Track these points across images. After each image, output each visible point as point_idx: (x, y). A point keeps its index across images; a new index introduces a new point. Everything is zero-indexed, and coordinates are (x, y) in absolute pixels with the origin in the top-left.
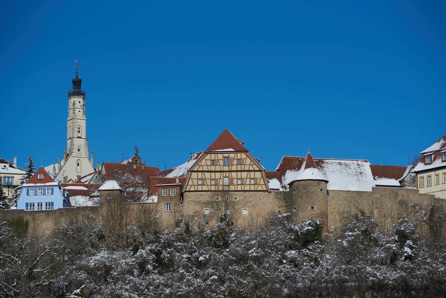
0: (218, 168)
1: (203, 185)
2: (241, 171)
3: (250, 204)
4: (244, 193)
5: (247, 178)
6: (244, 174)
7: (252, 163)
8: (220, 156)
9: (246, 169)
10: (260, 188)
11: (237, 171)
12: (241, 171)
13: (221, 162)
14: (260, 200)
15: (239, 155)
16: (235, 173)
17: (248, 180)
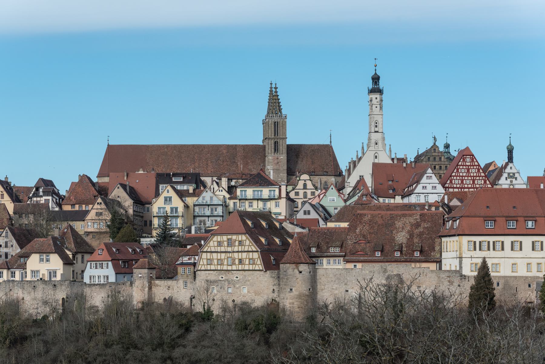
0: (223, 249)
1: (211, 264)
2: (241, 252)
3: (248, 283)
4: (243, 272)
5: (246, 258)
6: (244, 255)
7: (251, 244)
8: (225, 238)
9: (246, 249)
10: (257, 268)
11: (238, 252)
12: (241, 252)
13: (226, 244)
14: (257, 278)
15: (240, 236)
16: (237, 254)
17: (247, 260)
